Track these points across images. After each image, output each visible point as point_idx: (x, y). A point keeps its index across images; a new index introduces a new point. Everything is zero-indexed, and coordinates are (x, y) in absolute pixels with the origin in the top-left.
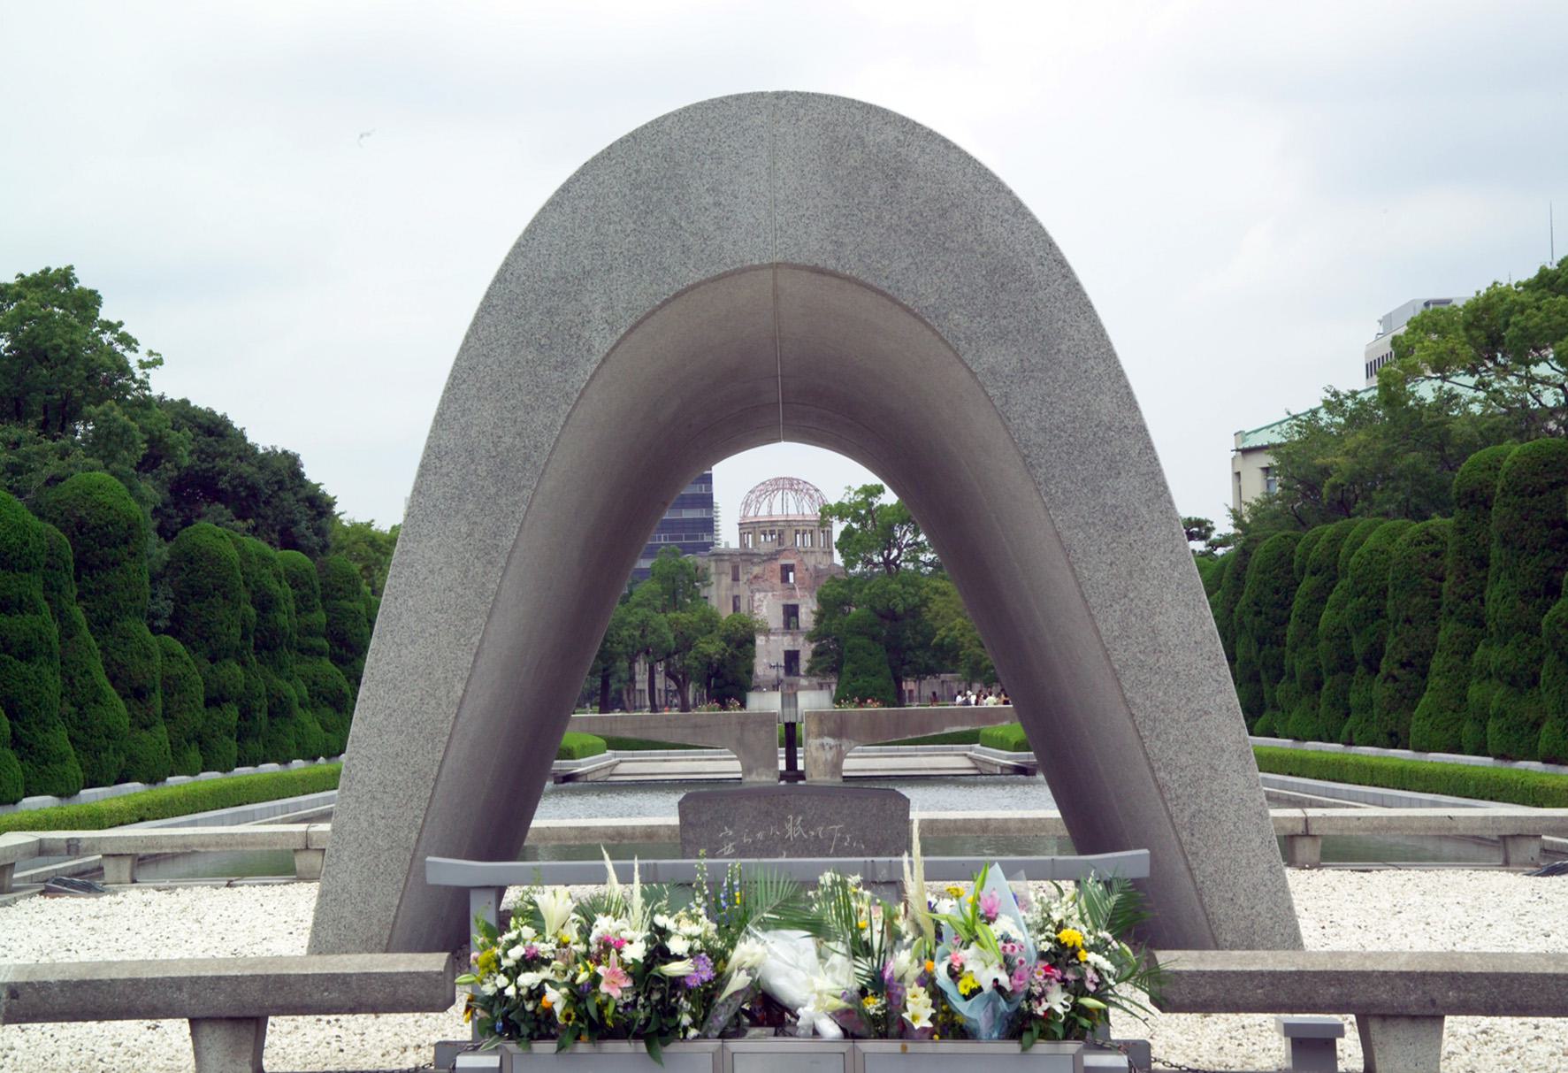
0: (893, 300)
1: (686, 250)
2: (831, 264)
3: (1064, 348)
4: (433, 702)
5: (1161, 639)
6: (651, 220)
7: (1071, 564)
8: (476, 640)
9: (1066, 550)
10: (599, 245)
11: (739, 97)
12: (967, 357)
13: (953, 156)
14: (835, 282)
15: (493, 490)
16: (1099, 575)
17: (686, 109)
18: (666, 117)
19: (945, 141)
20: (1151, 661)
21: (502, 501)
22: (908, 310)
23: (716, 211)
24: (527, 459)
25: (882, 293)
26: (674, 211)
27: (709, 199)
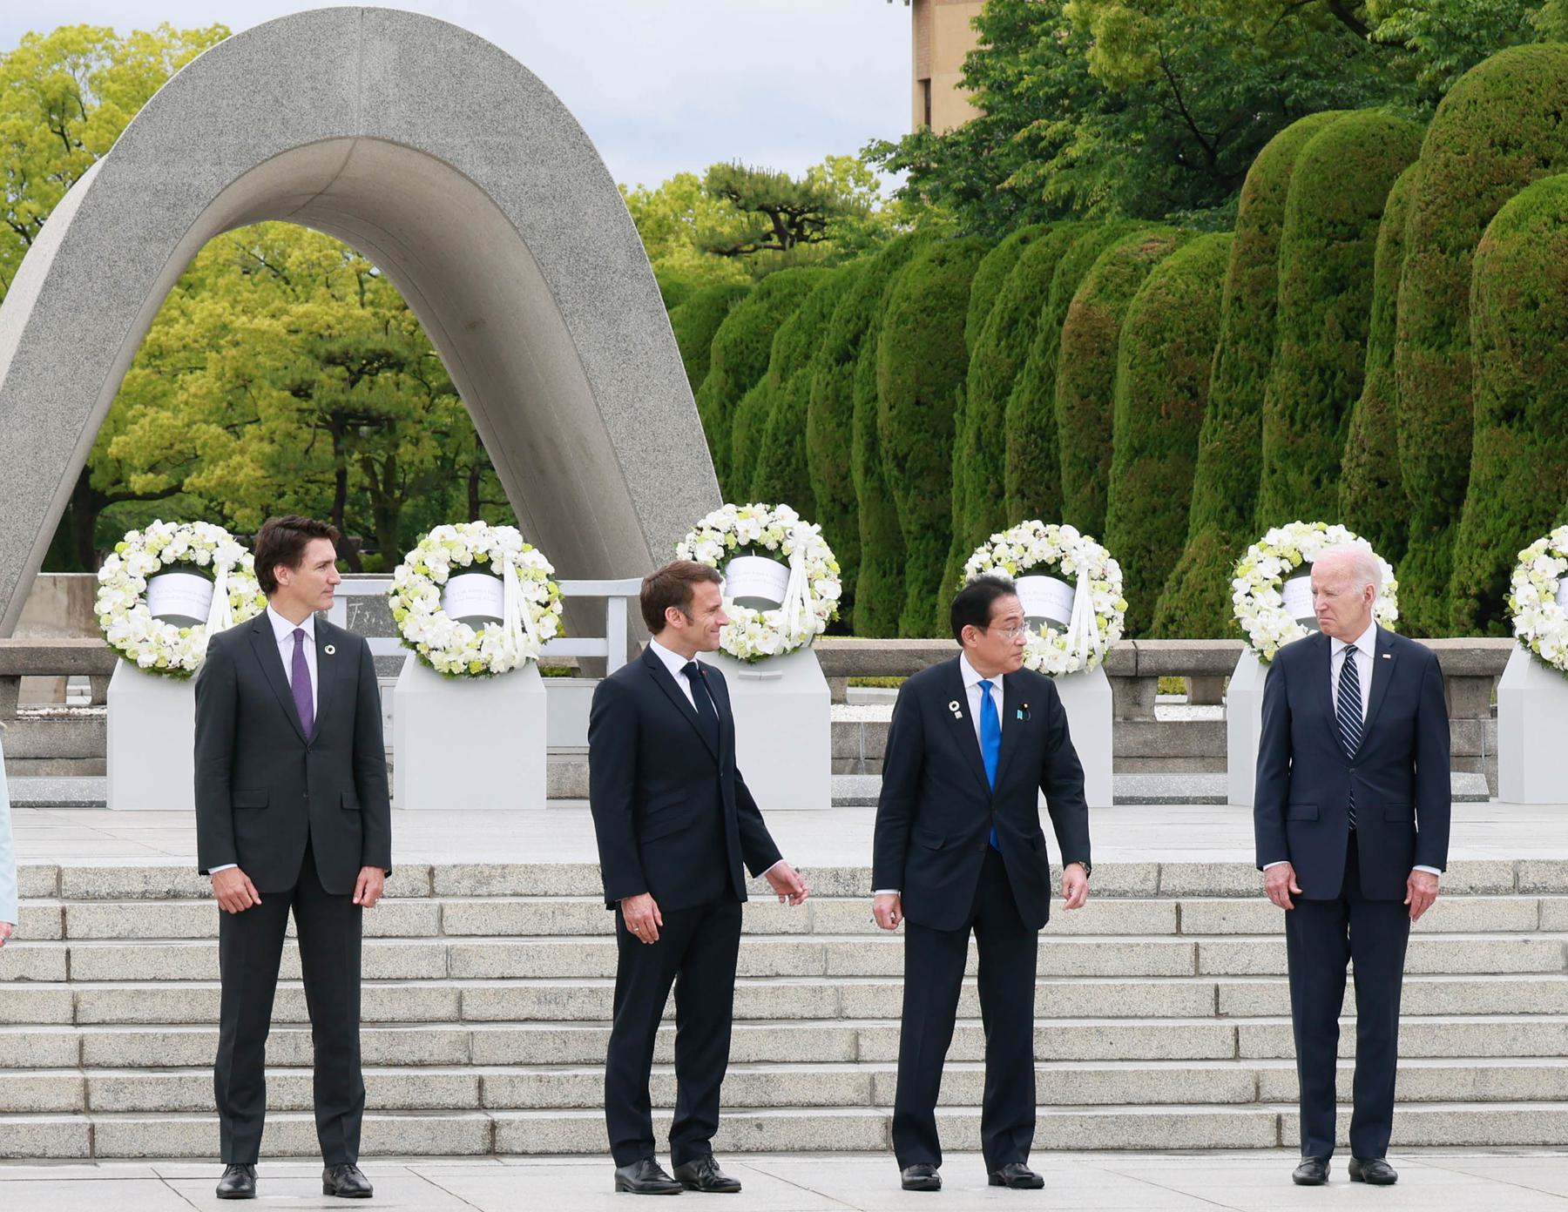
0: (454, 169)
1: (285, 122)
2: (405, 139)
3: (590, 211)
4: (37, 478)
5: (660, 441)
6: (258, 98)
7: (589, 380)
8: (79, 426)
9: (585, 368)
10: (213, 115)
11: (337, 10)
12: (512, 216)
13: (507, 63)
14: (405, 150)
15: (105, 304)
16: (611, 390)
17: (294, 16)
18: (277, 21)
19: (501, 52)
20: (651, 458)
21: (113, 314)
22: (463, 175)
23: (312, 94)
24: (137, 280)
25: (445, 163)
26: (278, 92)
27: (307, 84)
